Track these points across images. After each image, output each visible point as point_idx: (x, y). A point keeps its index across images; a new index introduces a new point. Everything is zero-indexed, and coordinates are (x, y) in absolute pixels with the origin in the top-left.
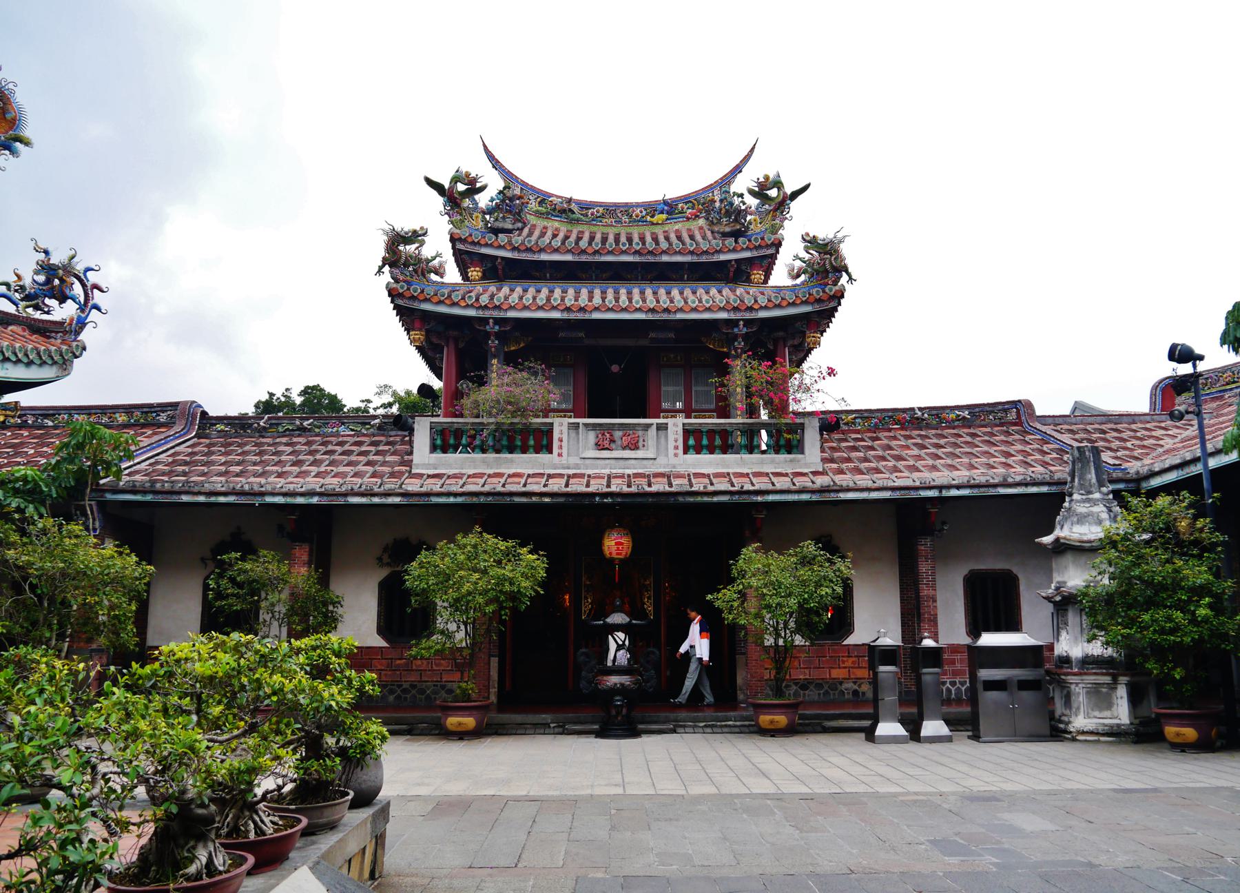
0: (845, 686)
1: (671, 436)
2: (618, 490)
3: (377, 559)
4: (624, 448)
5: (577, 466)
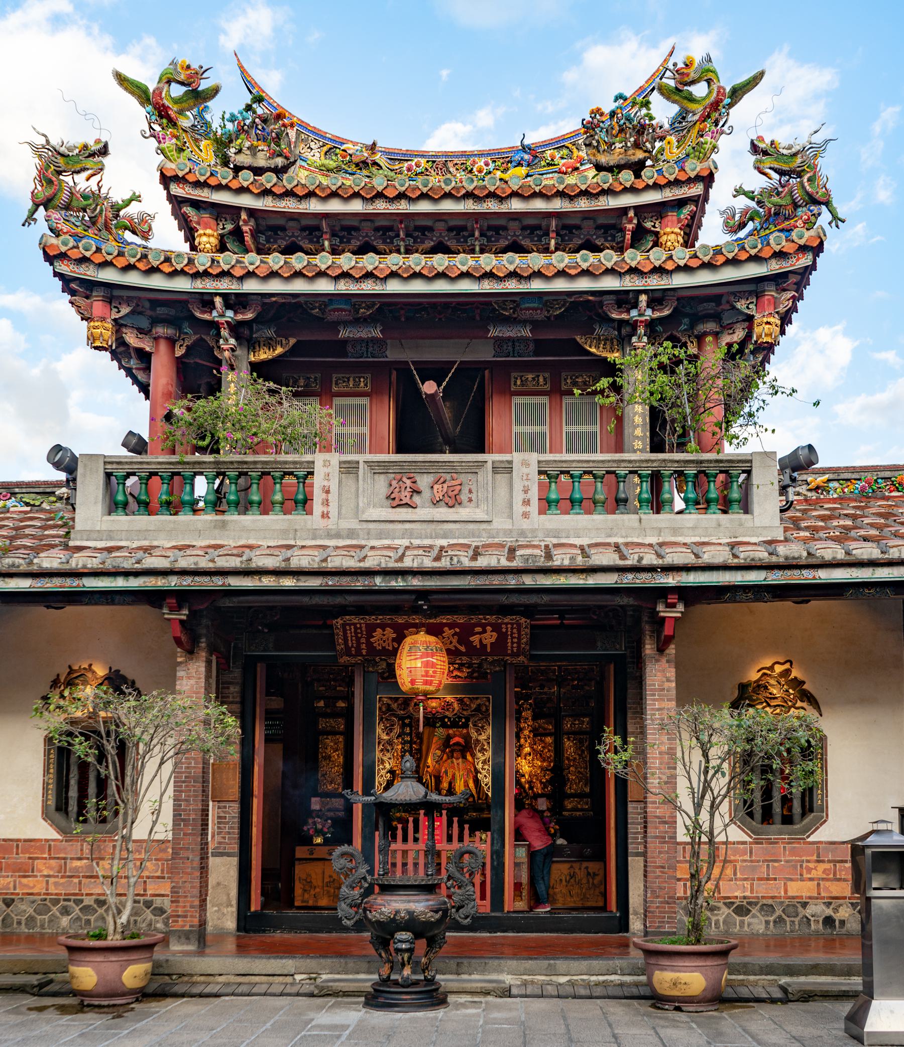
0: (809, 911)
2: (415, 565)
4: (435, 503)
5: (351, 534)
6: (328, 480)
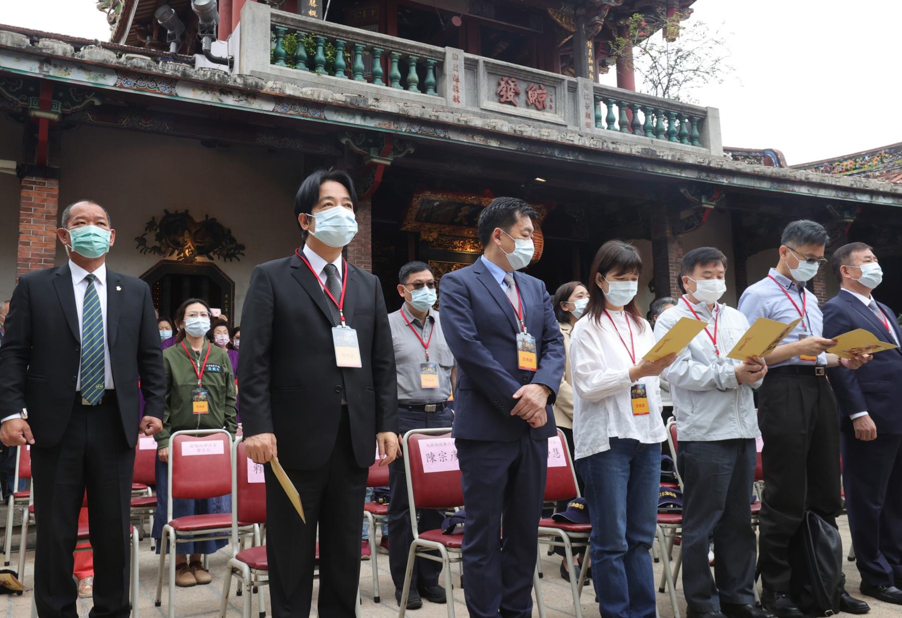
1: (582, 103)
3: (137, 239)
4: (528, 105)
6: (457, 71)
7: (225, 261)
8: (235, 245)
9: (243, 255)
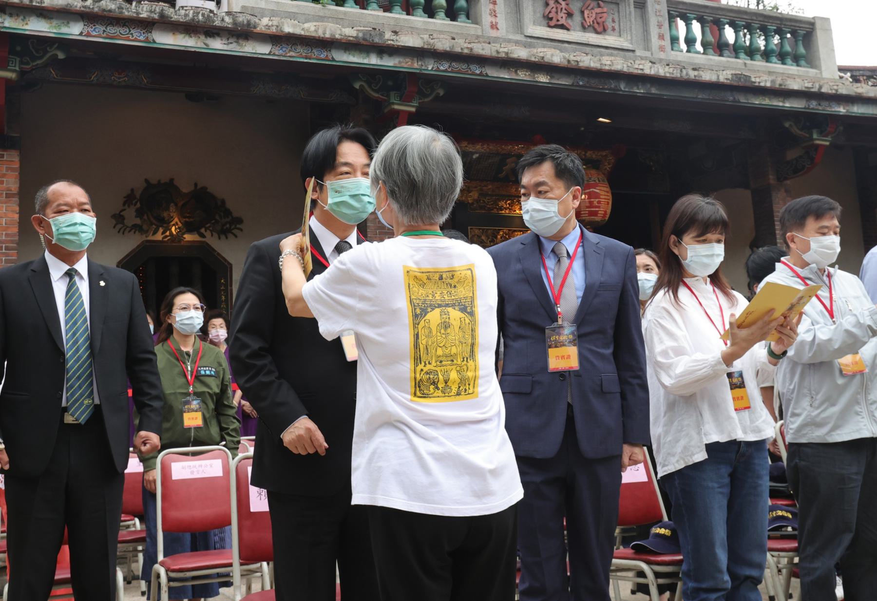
1: (653, 21)
3: (114, 216)
4: (584, 28)
7: (220, 238)
8: (230, 218)
9: (241, 230)
